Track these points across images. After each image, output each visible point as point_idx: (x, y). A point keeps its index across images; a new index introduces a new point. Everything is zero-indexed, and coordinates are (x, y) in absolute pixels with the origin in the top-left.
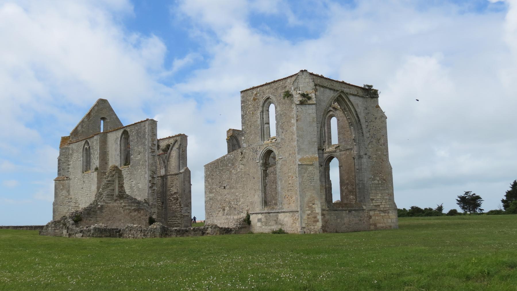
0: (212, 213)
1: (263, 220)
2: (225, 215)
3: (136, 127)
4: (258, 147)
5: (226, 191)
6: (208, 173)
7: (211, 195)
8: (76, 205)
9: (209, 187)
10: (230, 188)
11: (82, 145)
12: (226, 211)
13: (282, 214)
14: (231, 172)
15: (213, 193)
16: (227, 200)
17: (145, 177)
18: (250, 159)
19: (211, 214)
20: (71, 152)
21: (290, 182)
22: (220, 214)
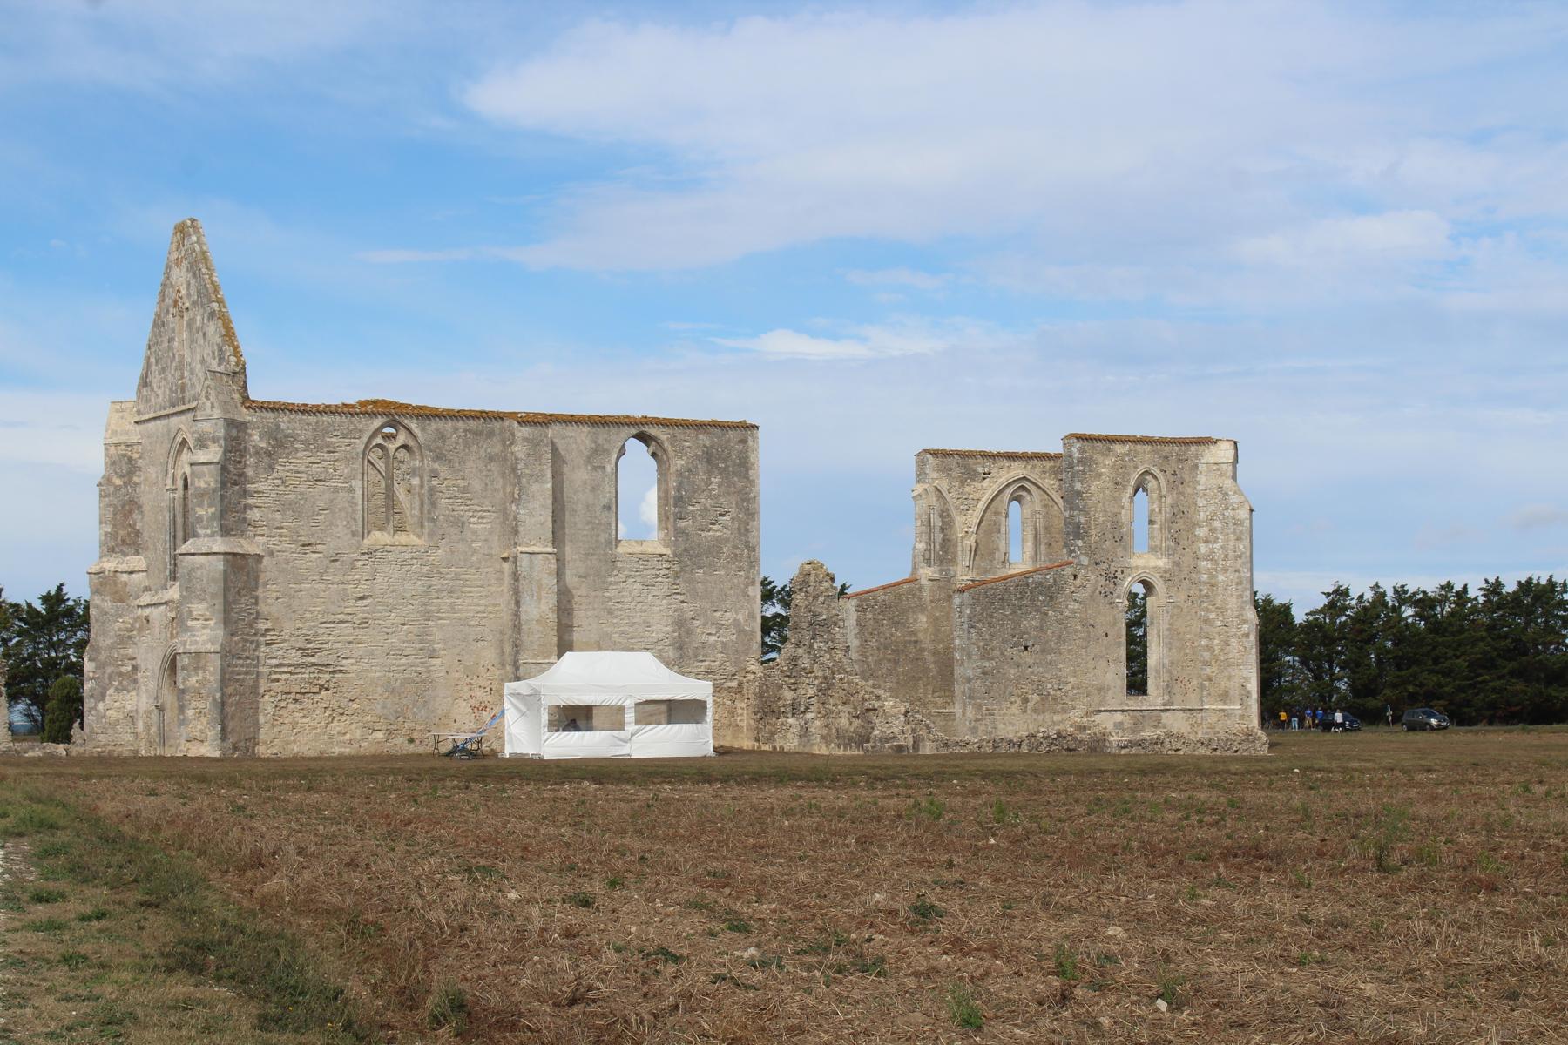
0: (989, 707)
1: (1126, 725)
2: (1029, 712)
3: (701, 437)
4: (1119, 570)
5: (1028, 658)
6: (978, 609)
7: (986, 664)
8: (312, 660)
9: (981, 644)
10: (1043, 651)
11: (360, 431)
12: (1030, 705)
13: (1168, 714)
14: (1046, 614)
15: (993, 659)
16: (1033, 677)
17: (746, 594)
18: (1098, 592)
19: (987, 710)
20: (263, 445)
21: (1188, 651)
22: (1015, 709)
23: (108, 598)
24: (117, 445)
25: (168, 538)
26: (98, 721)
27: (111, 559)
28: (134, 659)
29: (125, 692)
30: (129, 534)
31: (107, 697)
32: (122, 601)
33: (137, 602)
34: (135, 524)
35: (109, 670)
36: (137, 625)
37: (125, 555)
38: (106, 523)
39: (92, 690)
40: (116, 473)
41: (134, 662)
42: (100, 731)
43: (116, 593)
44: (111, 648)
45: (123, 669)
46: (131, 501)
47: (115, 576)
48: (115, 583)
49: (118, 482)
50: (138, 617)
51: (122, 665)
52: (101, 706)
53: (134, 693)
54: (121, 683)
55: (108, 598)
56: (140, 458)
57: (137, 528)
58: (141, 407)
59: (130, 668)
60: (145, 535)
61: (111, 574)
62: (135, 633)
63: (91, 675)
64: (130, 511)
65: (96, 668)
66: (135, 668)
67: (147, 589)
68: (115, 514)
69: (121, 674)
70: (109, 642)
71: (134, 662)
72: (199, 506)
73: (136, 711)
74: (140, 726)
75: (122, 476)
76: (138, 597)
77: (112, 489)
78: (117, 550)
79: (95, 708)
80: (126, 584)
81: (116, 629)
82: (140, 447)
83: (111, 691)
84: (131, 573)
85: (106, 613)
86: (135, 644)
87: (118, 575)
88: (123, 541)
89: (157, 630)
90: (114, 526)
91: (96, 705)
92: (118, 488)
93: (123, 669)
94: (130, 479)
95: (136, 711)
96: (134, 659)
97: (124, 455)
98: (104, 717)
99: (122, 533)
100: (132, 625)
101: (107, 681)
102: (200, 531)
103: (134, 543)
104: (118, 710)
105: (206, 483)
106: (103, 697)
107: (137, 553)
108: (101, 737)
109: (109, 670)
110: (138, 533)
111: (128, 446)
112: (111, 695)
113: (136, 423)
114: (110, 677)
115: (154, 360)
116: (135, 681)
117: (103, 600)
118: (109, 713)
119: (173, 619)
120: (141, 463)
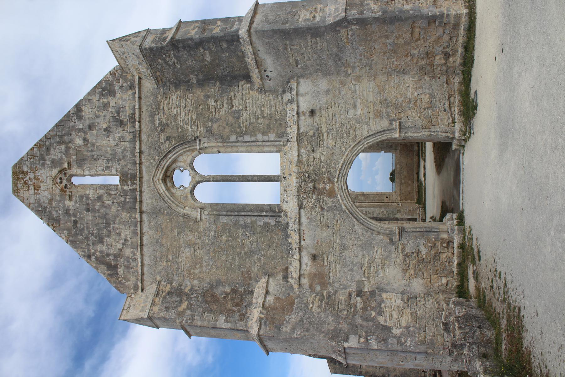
23: (287, 318)
24: (153, 304)
25: (242, 220)
26: (412, 335)
27: (251, 317)
28: (350, 294)
29: (383, 305)
30: (233, 299)
31: (388, 325)
32: (292, 303)
33: (296, 286)
34: (225, 293)
35: (359, 321)
36: (318, 288)
37: (250, 303)
38: (217, 321)
39: (378, 340)
40: (176, 307)
41: (354, 295)
42: (423, 334)
43: (283, 309)
44: (337, 317)
45: (359, 306)
46: (204, 295)
47: (267, 309)
48: (274, 309)
49: (185, 305)
50: (311, 286)
51: (356, 306)
52: (396, 331)
53: (384, 296)
54: (373, 309)
55: (287, 318)
56: (171, 284)
57: (229, 291)
58: (131, 284)
59: (359, 299)
60: (237, 277)
61: (265, 312)
62: (325, 292)
63: (362, 340)
64: (213, 296)
65: (356, 334)
66: (360, 293)
67: (285, 278)
68: (211, 311)
69: (364, 308)
70: (330, 319)
71: (354, 295)
72: (212, 31)
73: (403, 293)
74: (417, 286)
75: (181, 302)
76: (292, 287)
77: (189, 312)
78: (244, 311)
79: (398, 338)
80: (277, 298)
81: (319, 310)
82: (163, 283)
83: (381, 320)
84: (267, 292)
85: (302, 320)
86: (336, 292)
87: (267, 305)
88: (238, 305)
89: (325, 234)
90: (221, 313)
91: (395, 337)
92: (190, 307)
93: (359, 306)
94: (186, 294)
95: (403, 293)
96: (350, 294)
97: (165, 298)
98: (407, 328)
99: (229, 306)
100: (317, 294)
101: (370, 323)
102: (234, 28)
103: (242, 295)
104: (401, 314)
105: (194, 29)
106: (387, 329)
107: (252, 292)
108: (430, 334)
109: (359, 321)
110: (234, 291)
111: (157, 295)
112: (385, 320)
113: (142, 290)
114: (366, 319)
115: (99, 247)
116: (373, 293)
117: (288, 323)
118: (403, 325)
119: (315, 188)
120: (175, 284)
